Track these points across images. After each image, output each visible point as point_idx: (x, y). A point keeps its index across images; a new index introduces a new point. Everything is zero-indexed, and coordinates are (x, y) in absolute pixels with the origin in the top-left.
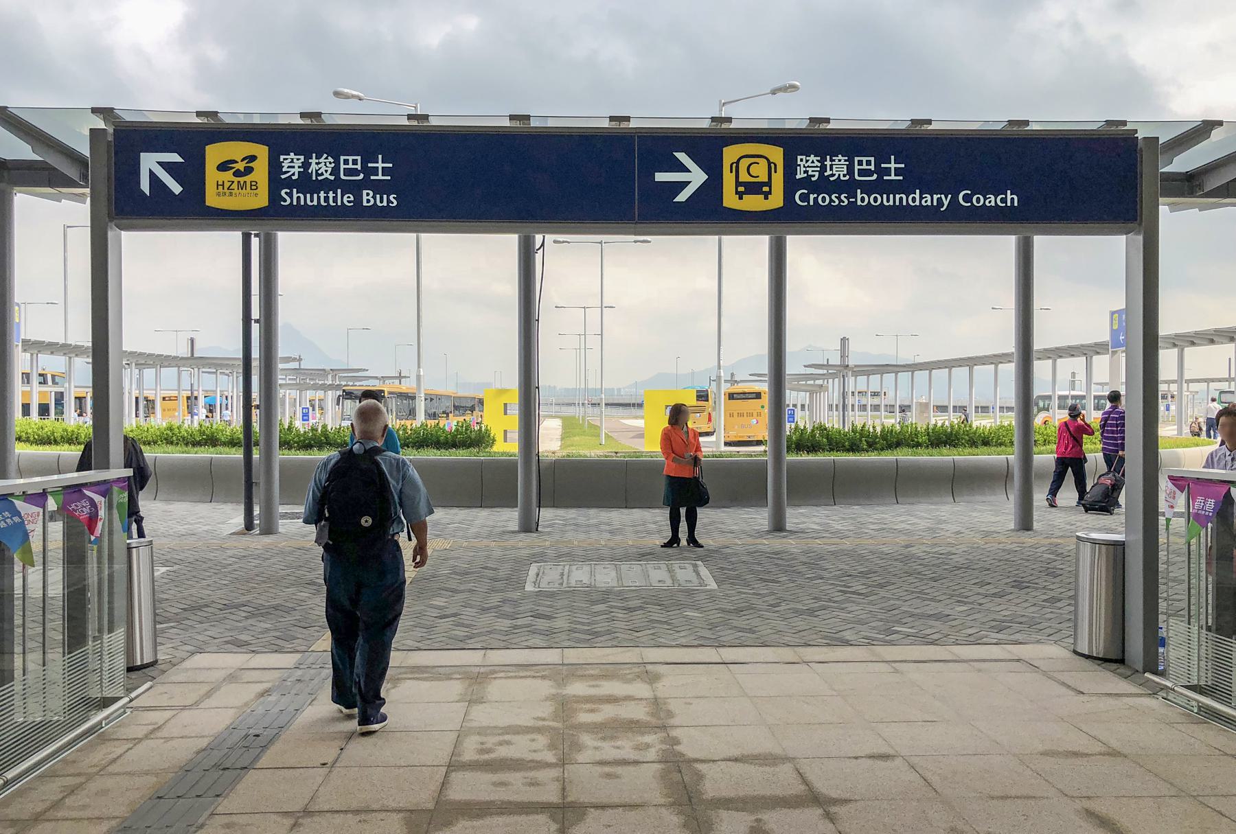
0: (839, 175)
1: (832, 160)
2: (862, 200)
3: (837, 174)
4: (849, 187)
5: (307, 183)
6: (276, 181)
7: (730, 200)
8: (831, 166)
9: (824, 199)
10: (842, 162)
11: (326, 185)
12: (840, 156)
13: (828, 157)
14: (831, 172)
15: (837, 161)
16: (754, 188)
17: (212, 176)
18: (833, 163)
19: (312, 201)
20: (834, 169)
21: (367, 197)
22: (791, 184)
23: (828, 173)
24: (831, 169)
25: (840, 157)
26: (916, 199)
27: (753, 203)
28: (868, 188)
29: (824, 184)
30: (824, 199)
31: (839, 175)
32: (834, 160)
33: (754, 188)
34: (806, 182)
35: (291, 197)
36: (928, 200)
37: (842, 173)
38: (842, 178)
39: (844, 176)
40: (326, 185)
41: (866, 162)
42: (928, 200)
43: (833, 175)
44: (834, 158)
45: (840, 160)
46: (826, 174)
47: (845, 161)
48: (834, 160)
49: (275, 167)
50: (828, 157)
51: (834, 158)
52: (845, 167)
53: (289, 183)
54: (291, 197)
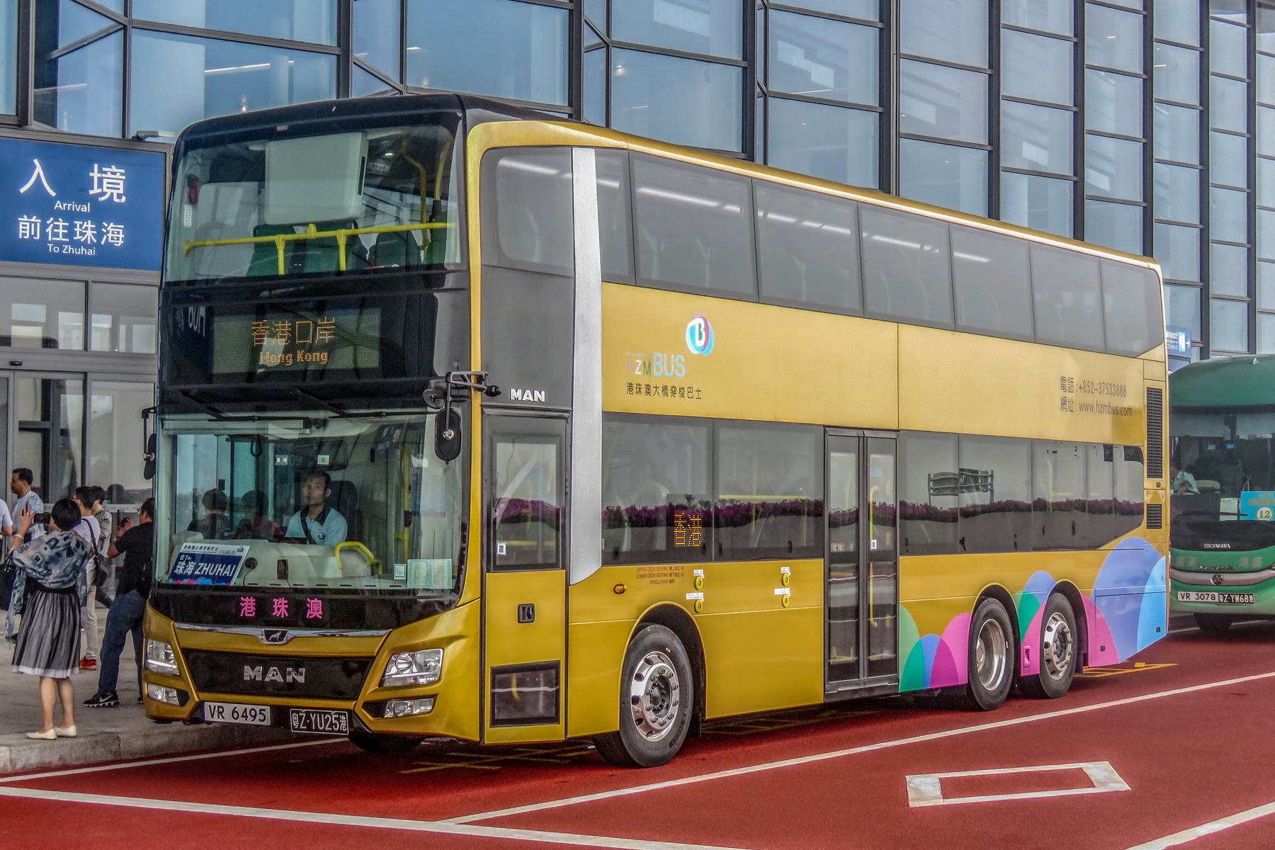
0: (112, 194)
1: (100, 171)
3: (109, 191)
8: (100, 180)
10: (118, 176)
12: (113, 167)
13: (96, 166)
14: (100, 190)
18: (103, 175)
20: (105, 185)
23: (96, 190)
24: (100, 185)
25: (114, 169)
31: (112, 194)
32: (106, 173)
38: (116, 200)
39: (119, 196)
43: (103, 194)
44: (104, 169)
45: (114, 173)
46: (91, 192)
47: (122, 174)
48: (106, 173)
50: (96, 166)
51: (104, 169)
52: (121, 183)
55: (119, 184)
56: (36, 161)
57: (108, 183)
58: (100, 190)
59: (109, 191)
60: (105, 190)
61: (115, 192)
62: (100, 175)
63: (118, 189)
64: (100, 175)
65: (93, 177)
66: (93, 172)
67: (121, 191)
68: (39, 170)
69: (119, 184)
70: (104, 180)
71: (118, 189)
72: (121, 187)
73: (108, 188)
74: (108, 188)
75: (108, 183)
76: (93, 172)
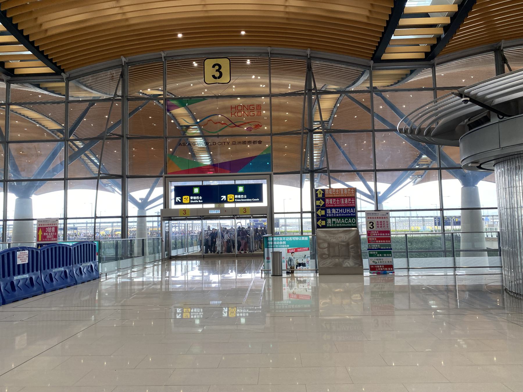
2: (242, 200)
4: (241, 199)
5: (193, 200)
6: (190, 200)
7: (228, 200)
9: (238, 200)
11: (195, 200)
16: (231, 199)
17: (183, 199)
19: (194, 202)
21: (199, 201)
22: (235, 199)
26: (248, 200)
27: (231, 201)
28: (243, 199)
29: (238, 199)
30: (238, 200)
33: (231, 199)
34: (236, 198)
35: (192, 201)
36: (249, 200)
40: (195, 200)
41: (242, 196)
42: (249, 200)
49: (190, 198)
53: (191, 200)
54: (192, 201)
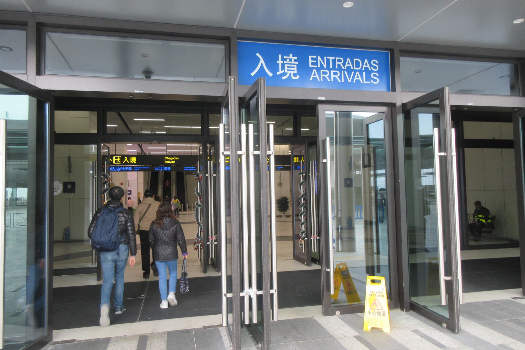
0: (290, 74)
1: (283, 59)
3: (289, 72)
8: (283, 65)
10: (293, 62)
13: (280, 56)
14: (283, 71)
15: (288, 60)
18: (285, 62)
20: (286, 68)
23: (280, 72)
24: (283, 68)
31: (290, 74)
32: (286, 60)
37: (292, 73)
38: (293, 77)
39: (295, 75)
43: (285, 74)
44: (285, 57)
45: (291, 60)
47: (295, 60)
48: (286, 60)
50: (280, 56)
51: (285, 57)
52: (295, 66)
55: (294, 67)
56: (258, 55)
57: (288, 67)
58: (283, 71)
59: (289, 72)
60: (286, 71)
61: (292, 73)
62: (282, 62)
63: (294, 70)
64: (282, 62)
65: (279, 63)
66: (279, 60)
67: (296, 72)
68: (262, 61)
69: (294, 67)
70: (285, 65)
71: (294, 70)
72: (295, 69)
73: (288, 70)
74: (288, 70)
75: (288, 67)
76: (279, 60)
